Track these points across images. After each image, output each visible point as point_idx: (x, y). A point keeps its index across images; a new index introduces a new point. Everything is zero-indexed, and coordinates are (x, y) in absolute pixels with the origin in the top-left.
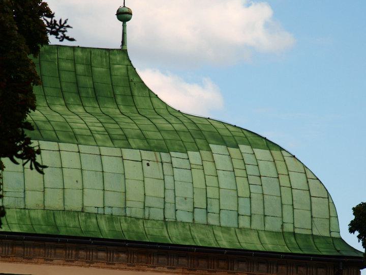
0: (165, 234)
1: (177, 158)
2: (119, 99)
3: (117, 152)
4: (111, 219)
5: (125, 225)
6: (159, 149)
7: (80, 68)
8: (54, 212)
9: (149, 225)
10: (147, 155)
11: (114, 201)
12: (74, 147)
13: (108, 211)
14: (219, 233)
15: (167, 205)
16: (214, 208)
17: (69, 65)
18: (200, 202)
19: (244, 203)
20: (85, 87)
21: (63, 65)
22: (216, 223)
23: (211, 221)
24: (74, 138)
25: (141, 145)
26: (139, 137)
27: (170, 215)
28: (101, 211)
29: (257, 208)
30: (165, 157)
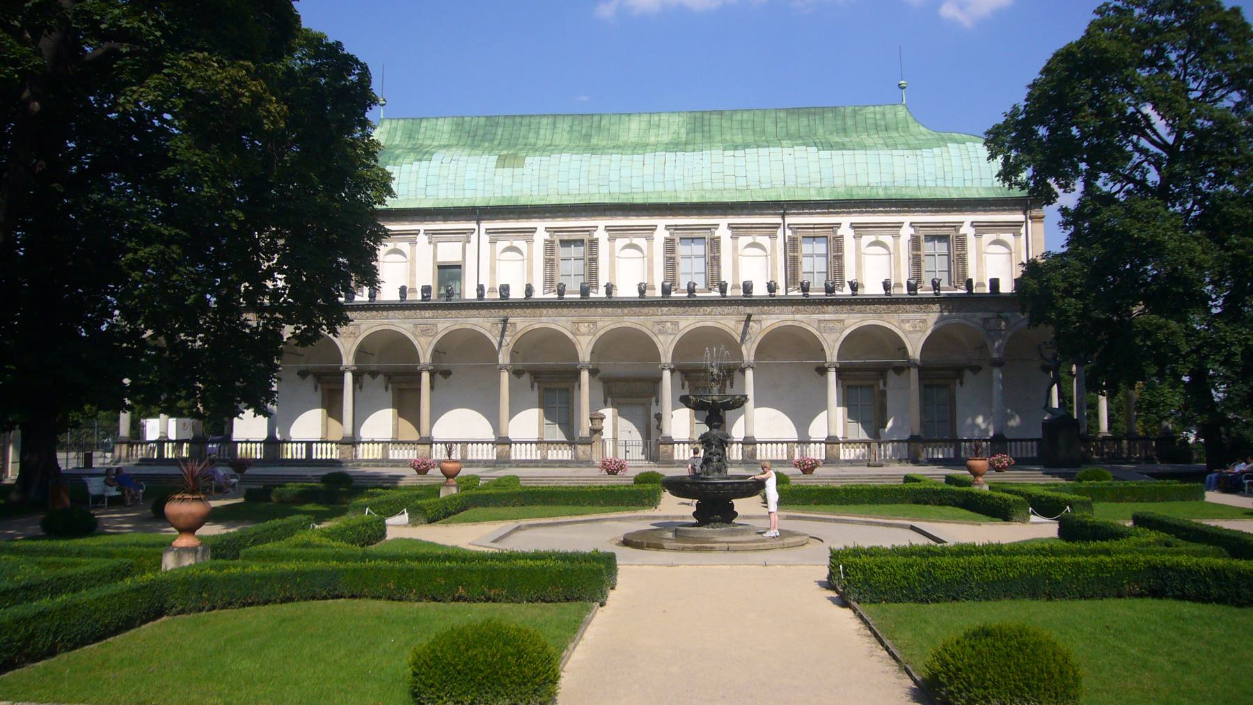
0: (919, 193)
1: (926, 152)
2: (900, 130)
3: (889, 152)
4: (886, 188)
5: (893, 191)
6: (916, 148)
7: (878, 117)
8: (851, 188)
9: (908, 190)
10: (906, 152)
11: (887, 179)
12: (864, 152)
13: (883, 184)
14: (952, 191)
15: (920, 179)
16: (949, 177)
17: (872, 116)
18: (940, 175)
19: (968, 174)
20: (881, 126)
21: (868, 116)
22: (950, 185)
23: (948, 185)
24: (864, 147)
25: (904, 147)
26: (904, 144)
27: (922, 183)
28: (879, 185)
29: (976, 175)
30: (918, 152)
